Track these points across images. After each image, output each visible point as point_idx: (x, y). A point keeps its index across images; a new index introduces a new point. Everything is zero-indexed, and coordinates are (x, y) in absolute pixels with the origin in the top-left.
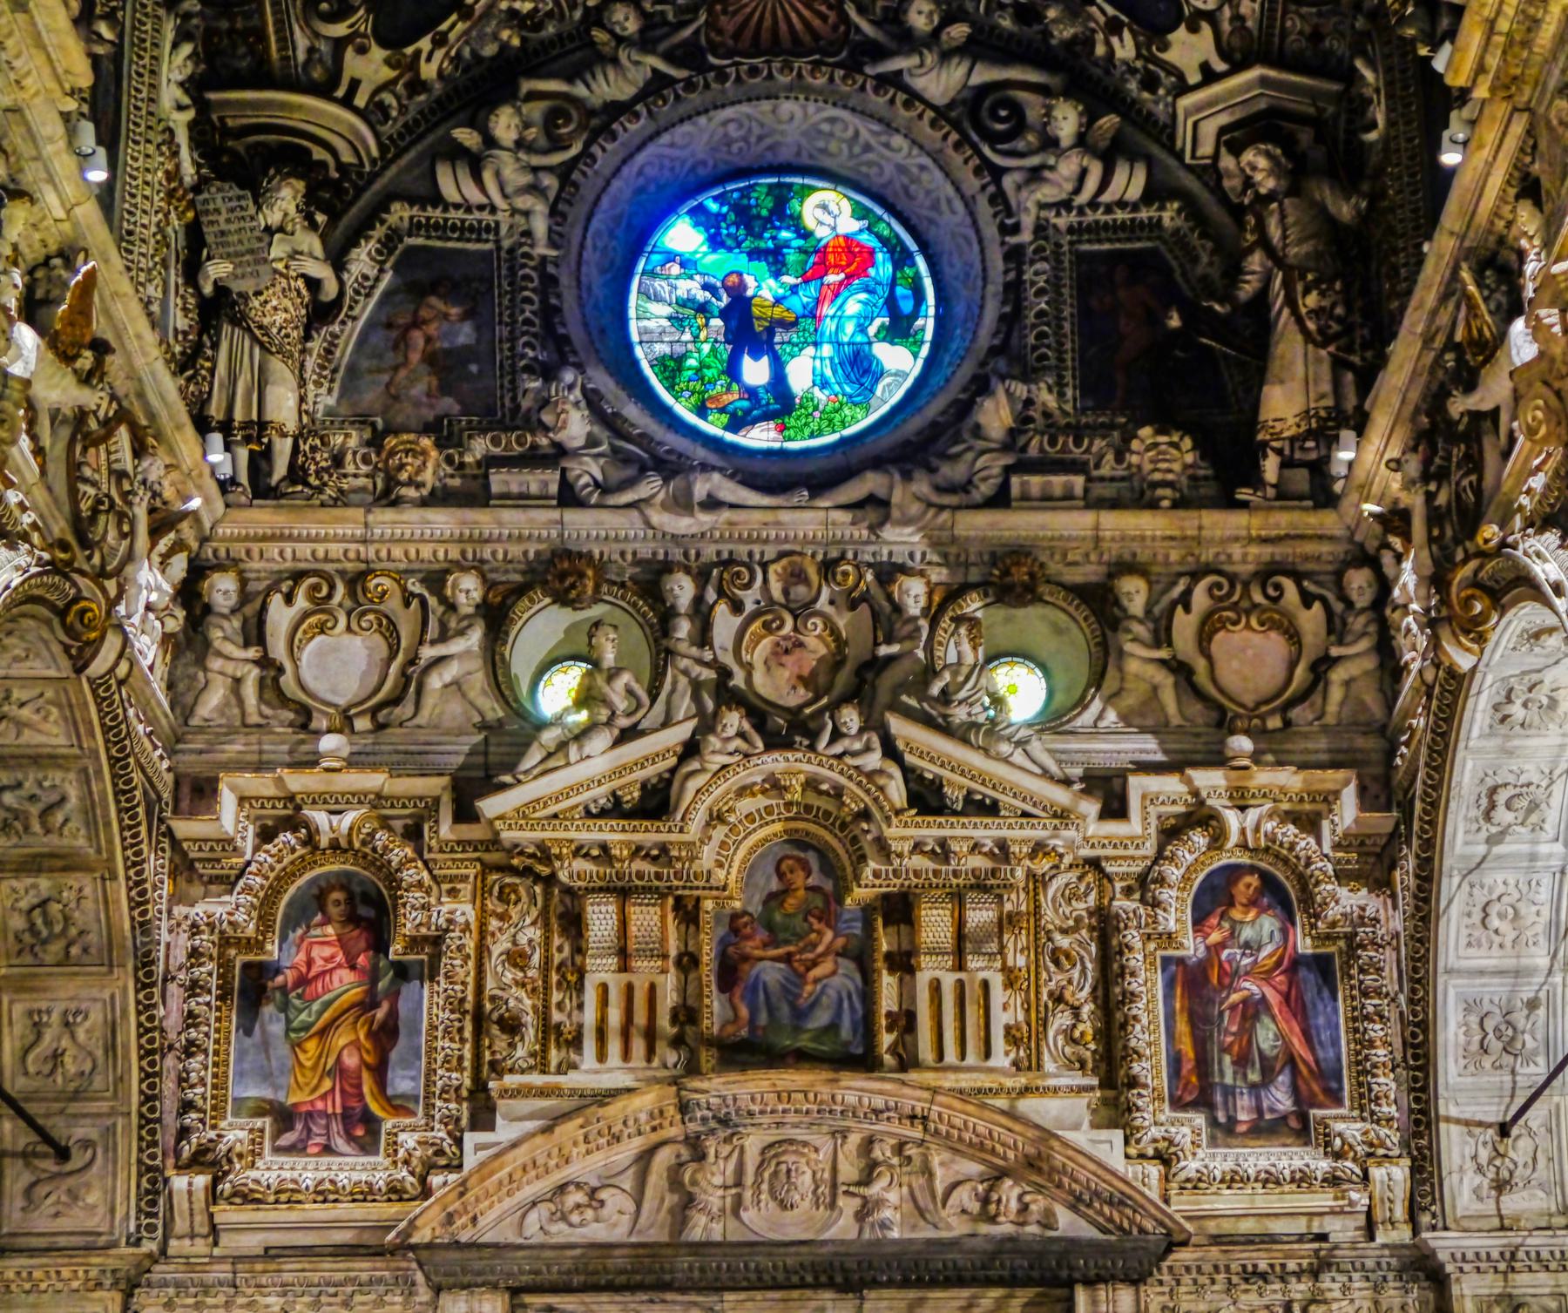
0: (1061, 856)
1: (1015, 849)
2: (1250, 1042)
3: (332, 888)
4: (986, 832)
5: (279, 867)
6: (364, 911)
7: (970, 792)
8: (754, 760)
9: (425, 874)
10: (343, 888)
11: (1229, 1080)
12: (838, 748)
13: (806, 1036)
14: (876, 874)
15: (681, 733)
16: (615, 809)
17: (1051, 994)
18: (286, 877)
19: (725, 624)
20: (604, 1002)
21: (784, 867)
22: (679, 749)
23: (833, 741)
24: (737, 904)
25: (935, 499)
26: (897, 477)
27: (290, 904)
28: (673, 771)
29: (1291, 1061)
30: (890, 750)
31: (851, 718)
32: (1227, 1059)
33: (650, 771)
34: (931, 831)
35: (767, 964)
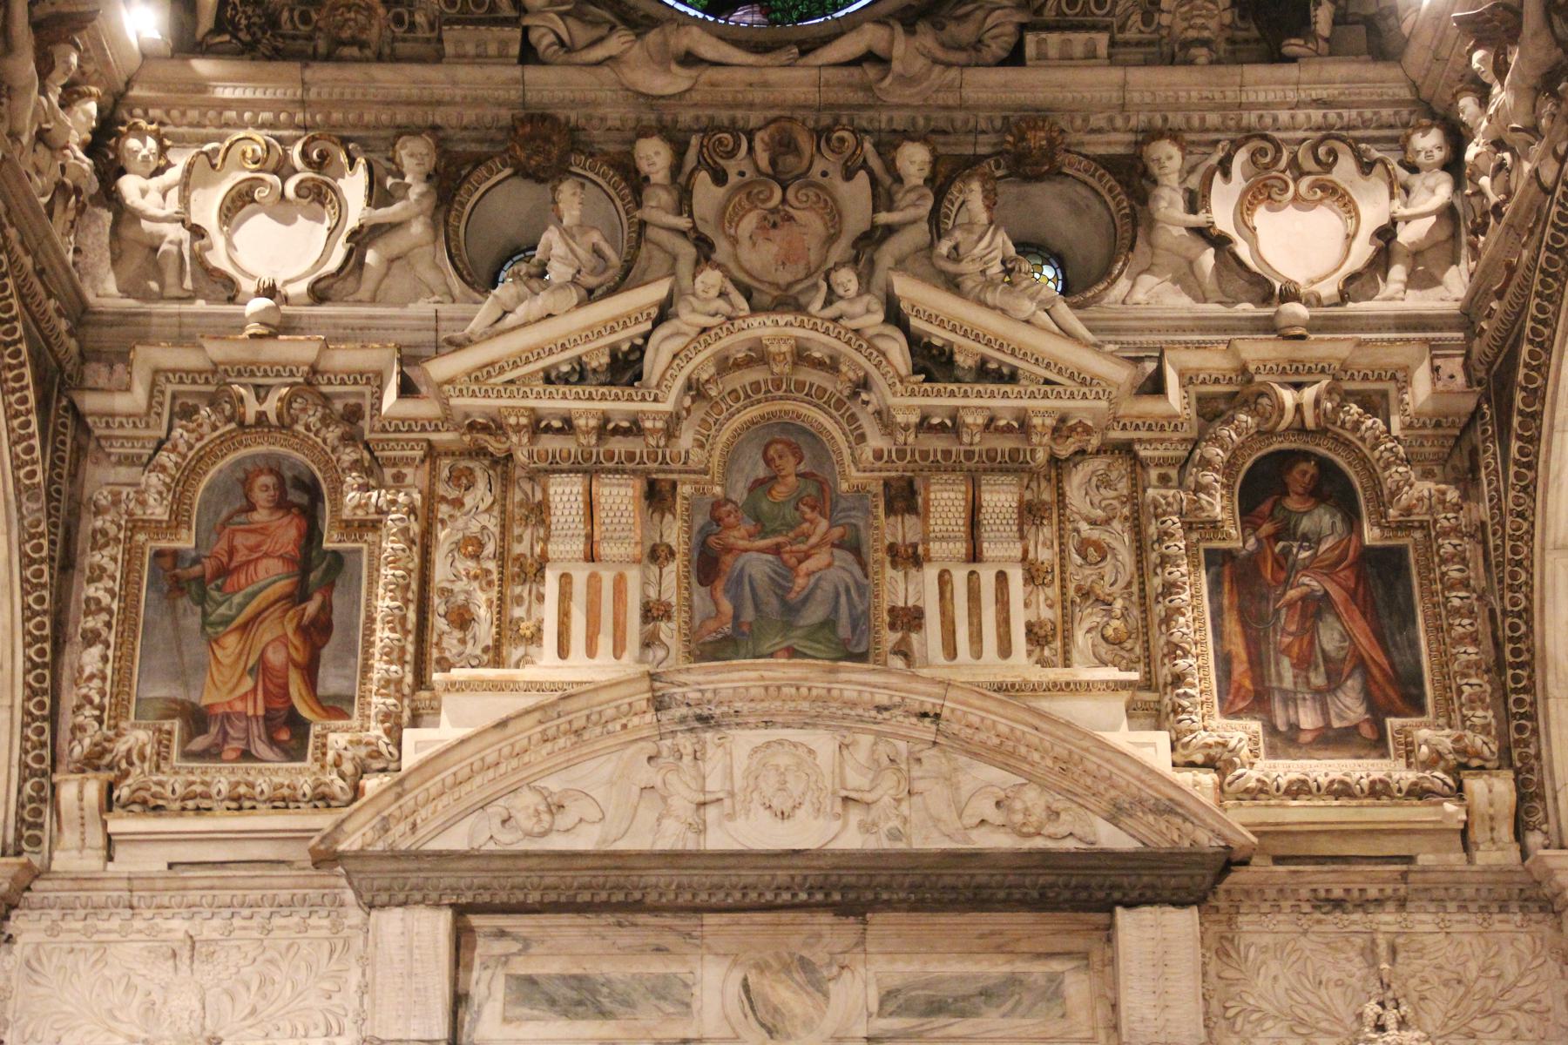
0: (1088, 430)
1: (1037, 421)
2: (1311, 643)
3: (261, 472)
4: (1002, 402)
5: (198, 445)
6: (295, 496)
7: (984, 361)
8: (738, 323)
9: (366, 455)
10: (271, 471)
11: (1288, 683)
12: (831, 312)
13: (799, 632)
14: (878, 455)
15: (656, 292)
16: (579, 374)
17: (1079, 589)
18: (205, 458)
19: (706, 194)
20: (565, 596)
21: (771, 452)
22: (654, 312)
23: (828, 303)
24: (718, 490)
25: (940, 54)
26: (899, 29)
27: (207, 489)
28: (646, 337)
29: (1361, 664)
30: (895, 315)
31: (847, 280)
32: (1286, 662)
33: (624, 337)
34: (940, 400)
35: (754, 555)
